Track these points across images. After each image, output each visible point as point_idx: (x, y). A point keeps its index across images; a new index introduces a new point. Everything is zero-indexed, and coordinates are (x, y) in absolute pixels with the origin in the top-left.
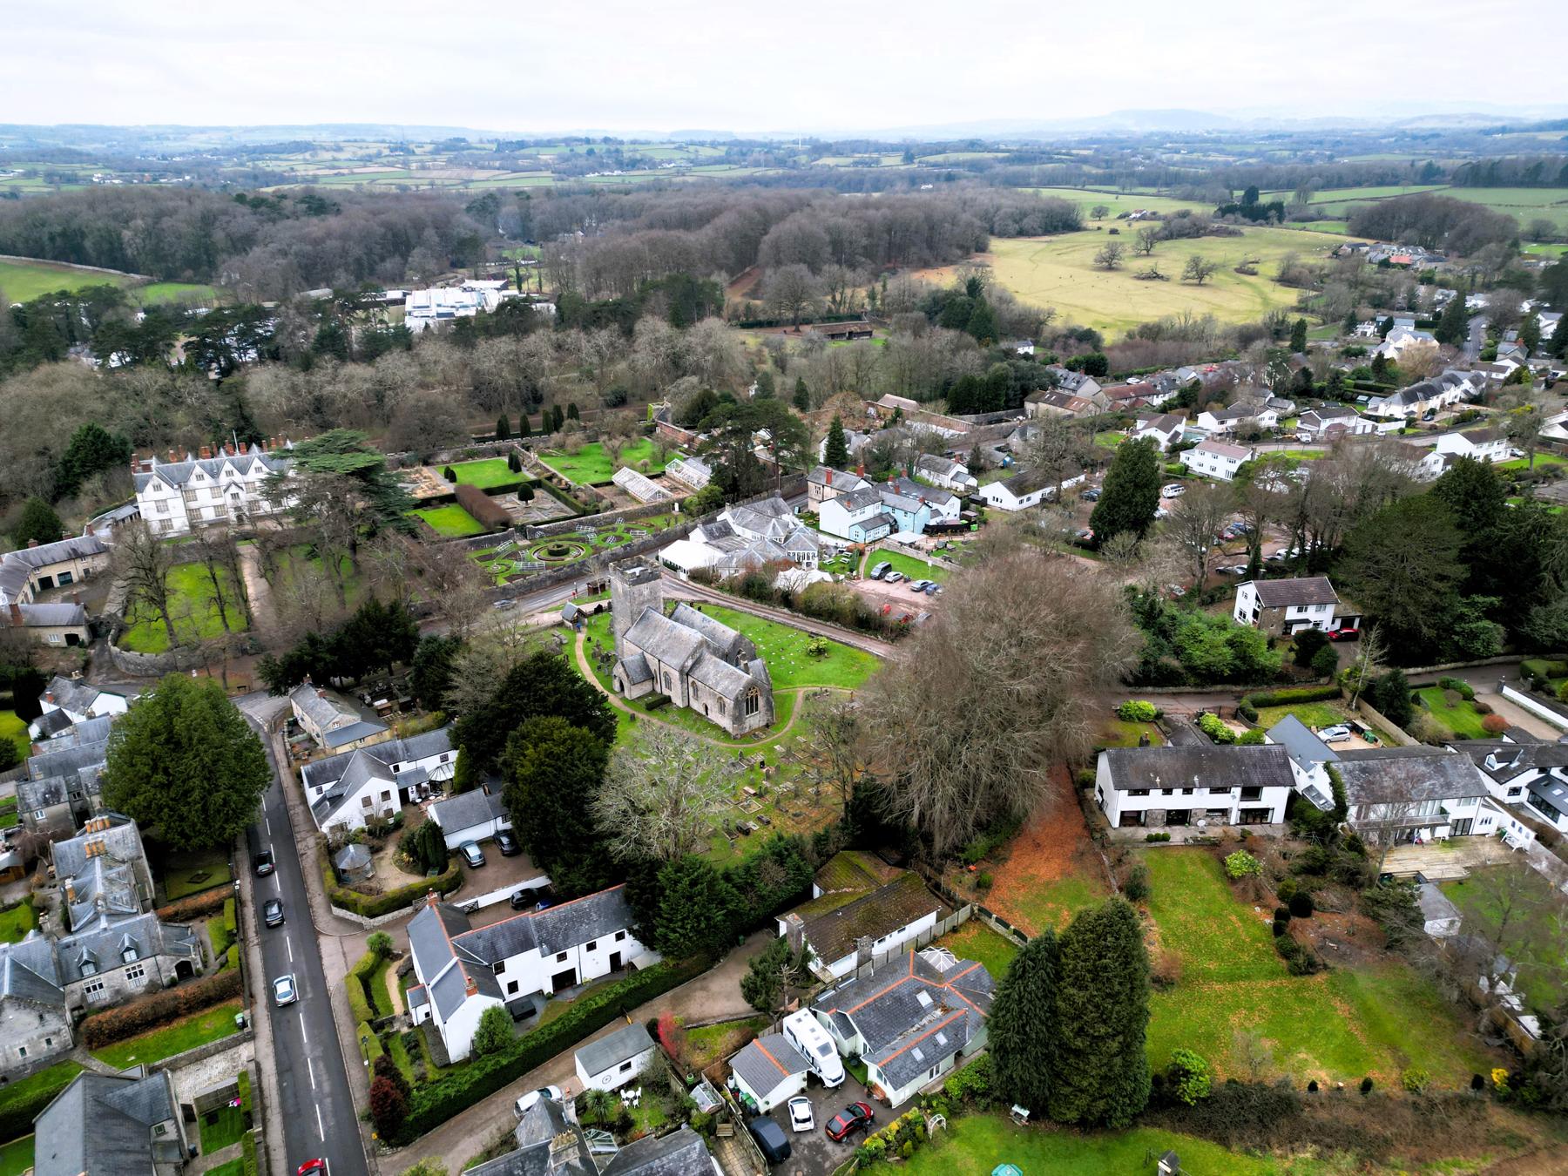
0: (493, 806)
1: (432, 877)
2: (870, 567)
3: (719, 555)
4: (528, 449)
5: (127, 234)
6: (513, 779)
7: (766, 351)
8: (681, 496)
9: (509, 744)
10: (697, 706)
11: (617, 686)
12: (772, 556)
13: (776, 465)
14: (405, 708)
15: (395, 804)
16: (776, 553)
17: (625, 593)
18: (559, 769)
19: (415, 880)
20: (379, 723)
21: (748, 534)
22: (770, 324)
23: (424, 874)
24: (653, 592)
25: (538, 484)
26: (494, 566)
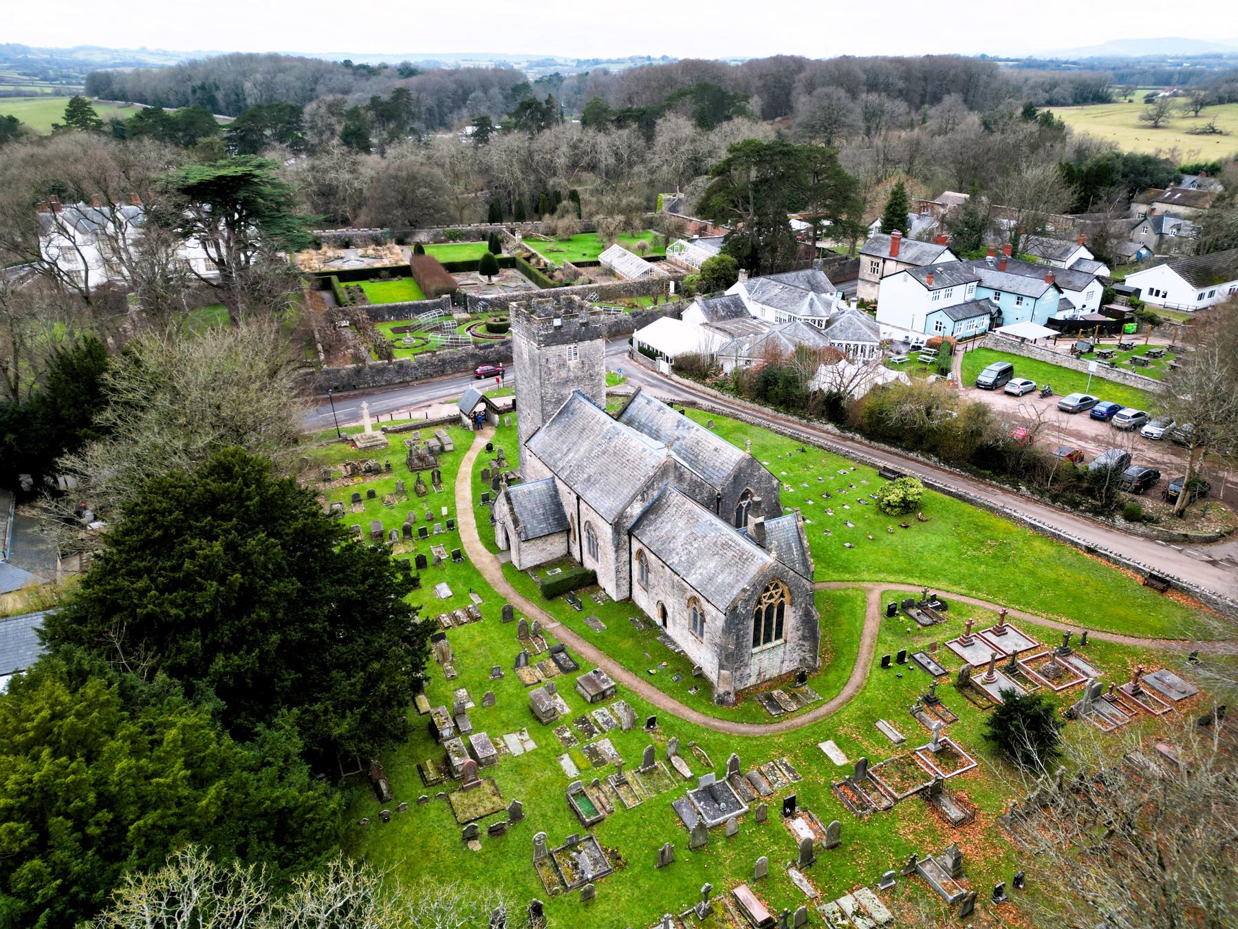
5: (248, 85)
10: (643, 600)
16: (812, 340)
21: (770, 314)
24: (587, 363)
25: (511, 263)
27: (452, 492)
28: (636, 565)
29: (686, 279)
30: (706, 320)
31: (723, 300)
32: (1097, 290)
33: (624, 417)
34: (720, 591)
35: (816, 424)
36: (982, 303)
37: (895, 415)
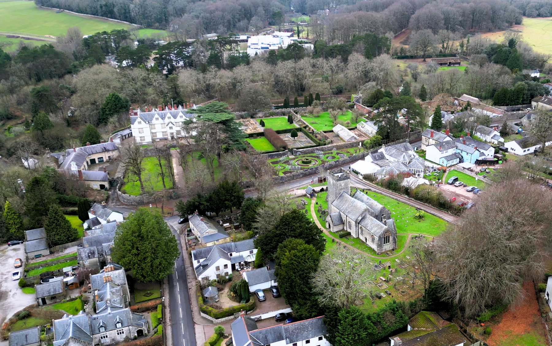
0: (270, 275)
1: (243, 304)
2: (448, 178)
3: (378, 168)
4: (297, 113)
6: (279, 265)
7: (409, 70)
8: (363, 139)
9: (278, 249)
10: (362, 238)
11: (327, 226)
12: (402, 170)
13: (408, 127)
14: (237, 228)
15: (229, 270)
16: (405, 169)
17: (333, 184)
18: (299, 263)
19: (235, 305)
20: (225, 234)
21: (392, 159)
22: (412, 57)
23: (240, 302)
24: (346, 185)
25: (300, 130)
26: (278, 167)
27: (311, 215)
28: (360, 230)
29: (365, 142)
30: (372, 161)
31: (378, 154)
32: (492, 150)
33: (354, 197)
34: (377, 233)
35: (403, 195)
36: (457, 154)
37: (420, 195)
